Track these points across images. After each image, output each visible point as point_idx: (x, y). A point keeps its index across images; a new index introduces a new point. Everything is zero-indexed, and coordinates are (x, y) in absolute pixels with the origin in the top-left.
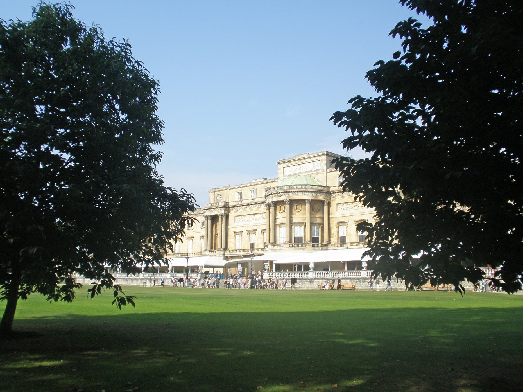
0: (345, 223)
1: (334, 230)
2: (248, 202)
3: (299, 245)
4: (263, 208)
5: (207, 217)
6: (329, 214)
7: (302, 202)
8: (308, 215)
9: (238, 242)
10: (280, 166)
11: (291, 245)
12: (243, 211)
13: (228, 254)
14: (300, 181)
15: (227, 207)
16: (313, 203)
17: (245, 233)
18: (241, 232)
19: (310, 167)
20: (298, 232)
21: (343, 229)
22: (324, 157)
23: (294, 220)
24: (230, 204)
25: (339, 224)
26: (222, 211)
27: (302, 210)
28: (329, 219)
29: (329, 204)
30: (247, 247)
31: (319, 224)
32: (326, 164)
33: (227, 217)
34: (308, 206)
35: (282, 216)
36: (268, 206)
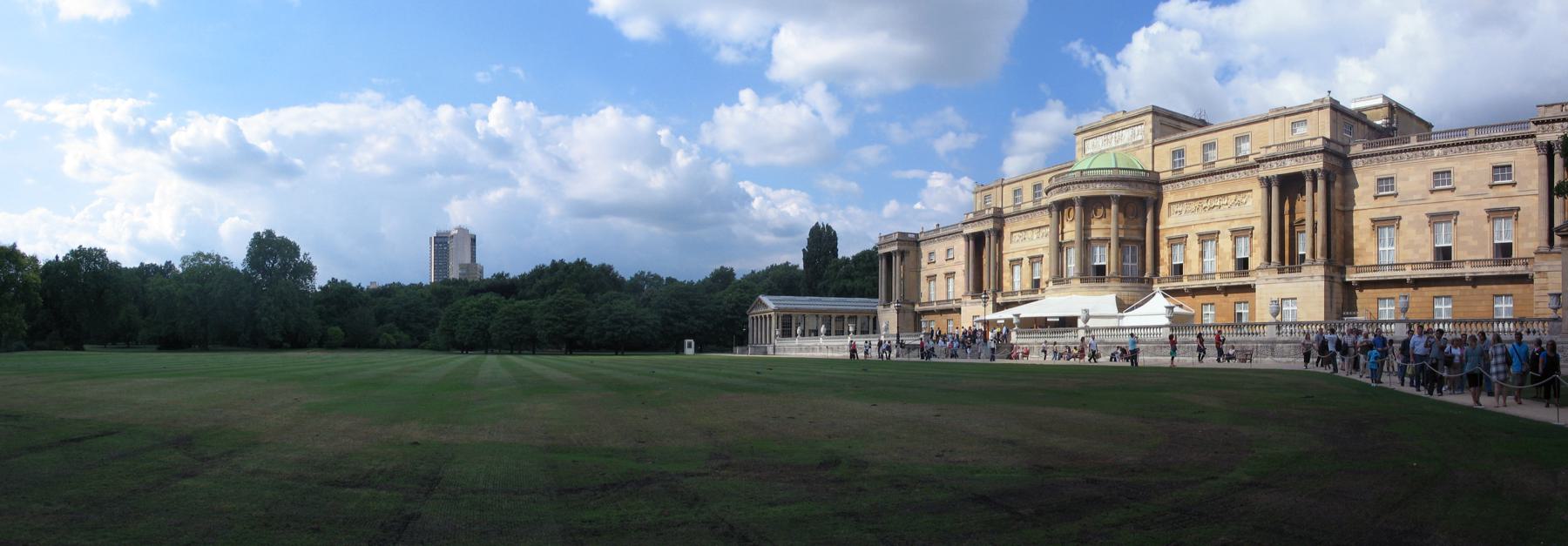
0: (1182, 240)
1: (1164, 252)
2: (1030, 206)
3: (1098, 281)
4: (1045, 218)
5: (967, 237)
6: (1156, 222)
7: (1103, 201)
8: (1113, 225)
9: (1017, 279)
10: (1079, 138)
11: (1082, 281)
12: (1022, 223)
13: (1000, 300)
14: (1106, 162)
15: (999, 217)
16: (1123, 202)
17: (1026, 261)
18: (1019, 261)
19: (1126, 136)
20: (1101, 257)
21: (1178, 250)
22: (1149, 117)
23: (1095, 235)
24: (1006, 211)
25: (1173, 242)
26: (988, 225)
27: (1104, 216)
28: (1156, 232)
29: (1157, 205)
30: (1028, 286)
31: (1137, 242)
32: (1153, 131)
33: (999, 234)
34: (1114, 207)
35: (1071, 230)
36: (1049, 208)
